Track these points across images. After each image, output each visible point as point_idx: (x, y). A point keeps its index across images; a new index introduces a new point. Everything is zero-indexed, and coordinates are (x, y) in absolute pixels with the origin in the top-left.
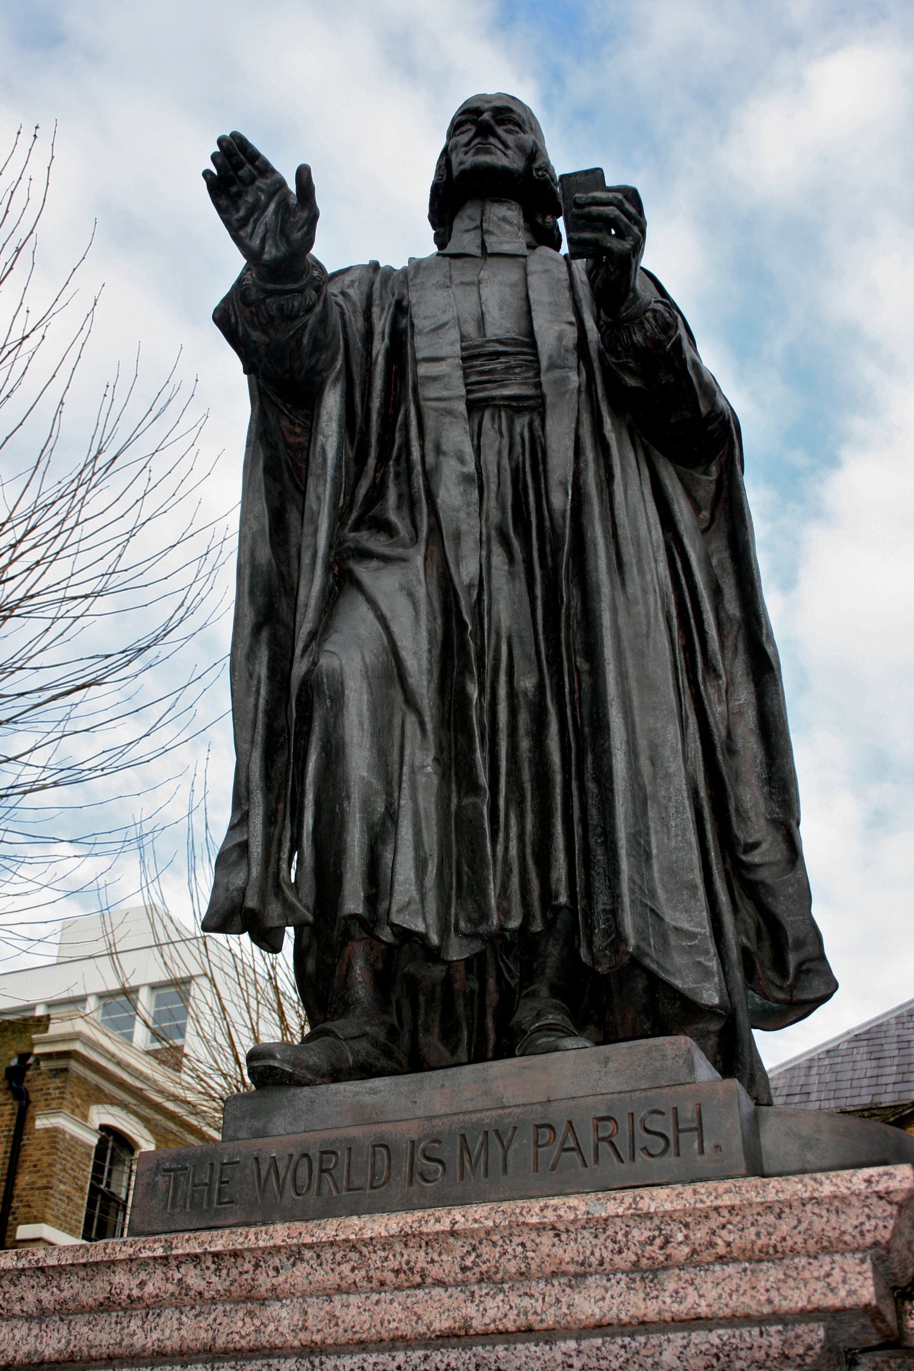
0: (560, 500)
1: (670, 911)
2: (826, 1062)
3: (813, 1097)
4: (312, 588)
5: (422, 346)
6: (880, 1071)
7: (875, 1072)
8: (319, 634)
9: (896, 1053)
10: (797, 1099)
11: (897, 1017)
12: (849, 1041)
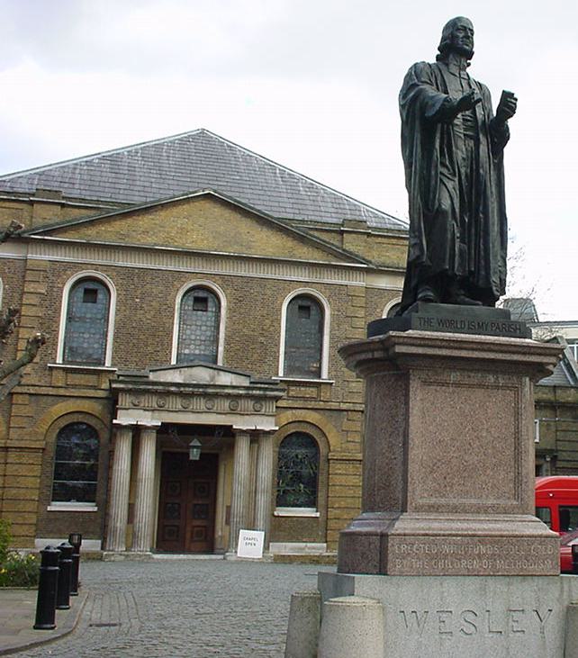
3: (77, 186)
6: (117, 181)
9: (126, 172)
11: (128, 152)
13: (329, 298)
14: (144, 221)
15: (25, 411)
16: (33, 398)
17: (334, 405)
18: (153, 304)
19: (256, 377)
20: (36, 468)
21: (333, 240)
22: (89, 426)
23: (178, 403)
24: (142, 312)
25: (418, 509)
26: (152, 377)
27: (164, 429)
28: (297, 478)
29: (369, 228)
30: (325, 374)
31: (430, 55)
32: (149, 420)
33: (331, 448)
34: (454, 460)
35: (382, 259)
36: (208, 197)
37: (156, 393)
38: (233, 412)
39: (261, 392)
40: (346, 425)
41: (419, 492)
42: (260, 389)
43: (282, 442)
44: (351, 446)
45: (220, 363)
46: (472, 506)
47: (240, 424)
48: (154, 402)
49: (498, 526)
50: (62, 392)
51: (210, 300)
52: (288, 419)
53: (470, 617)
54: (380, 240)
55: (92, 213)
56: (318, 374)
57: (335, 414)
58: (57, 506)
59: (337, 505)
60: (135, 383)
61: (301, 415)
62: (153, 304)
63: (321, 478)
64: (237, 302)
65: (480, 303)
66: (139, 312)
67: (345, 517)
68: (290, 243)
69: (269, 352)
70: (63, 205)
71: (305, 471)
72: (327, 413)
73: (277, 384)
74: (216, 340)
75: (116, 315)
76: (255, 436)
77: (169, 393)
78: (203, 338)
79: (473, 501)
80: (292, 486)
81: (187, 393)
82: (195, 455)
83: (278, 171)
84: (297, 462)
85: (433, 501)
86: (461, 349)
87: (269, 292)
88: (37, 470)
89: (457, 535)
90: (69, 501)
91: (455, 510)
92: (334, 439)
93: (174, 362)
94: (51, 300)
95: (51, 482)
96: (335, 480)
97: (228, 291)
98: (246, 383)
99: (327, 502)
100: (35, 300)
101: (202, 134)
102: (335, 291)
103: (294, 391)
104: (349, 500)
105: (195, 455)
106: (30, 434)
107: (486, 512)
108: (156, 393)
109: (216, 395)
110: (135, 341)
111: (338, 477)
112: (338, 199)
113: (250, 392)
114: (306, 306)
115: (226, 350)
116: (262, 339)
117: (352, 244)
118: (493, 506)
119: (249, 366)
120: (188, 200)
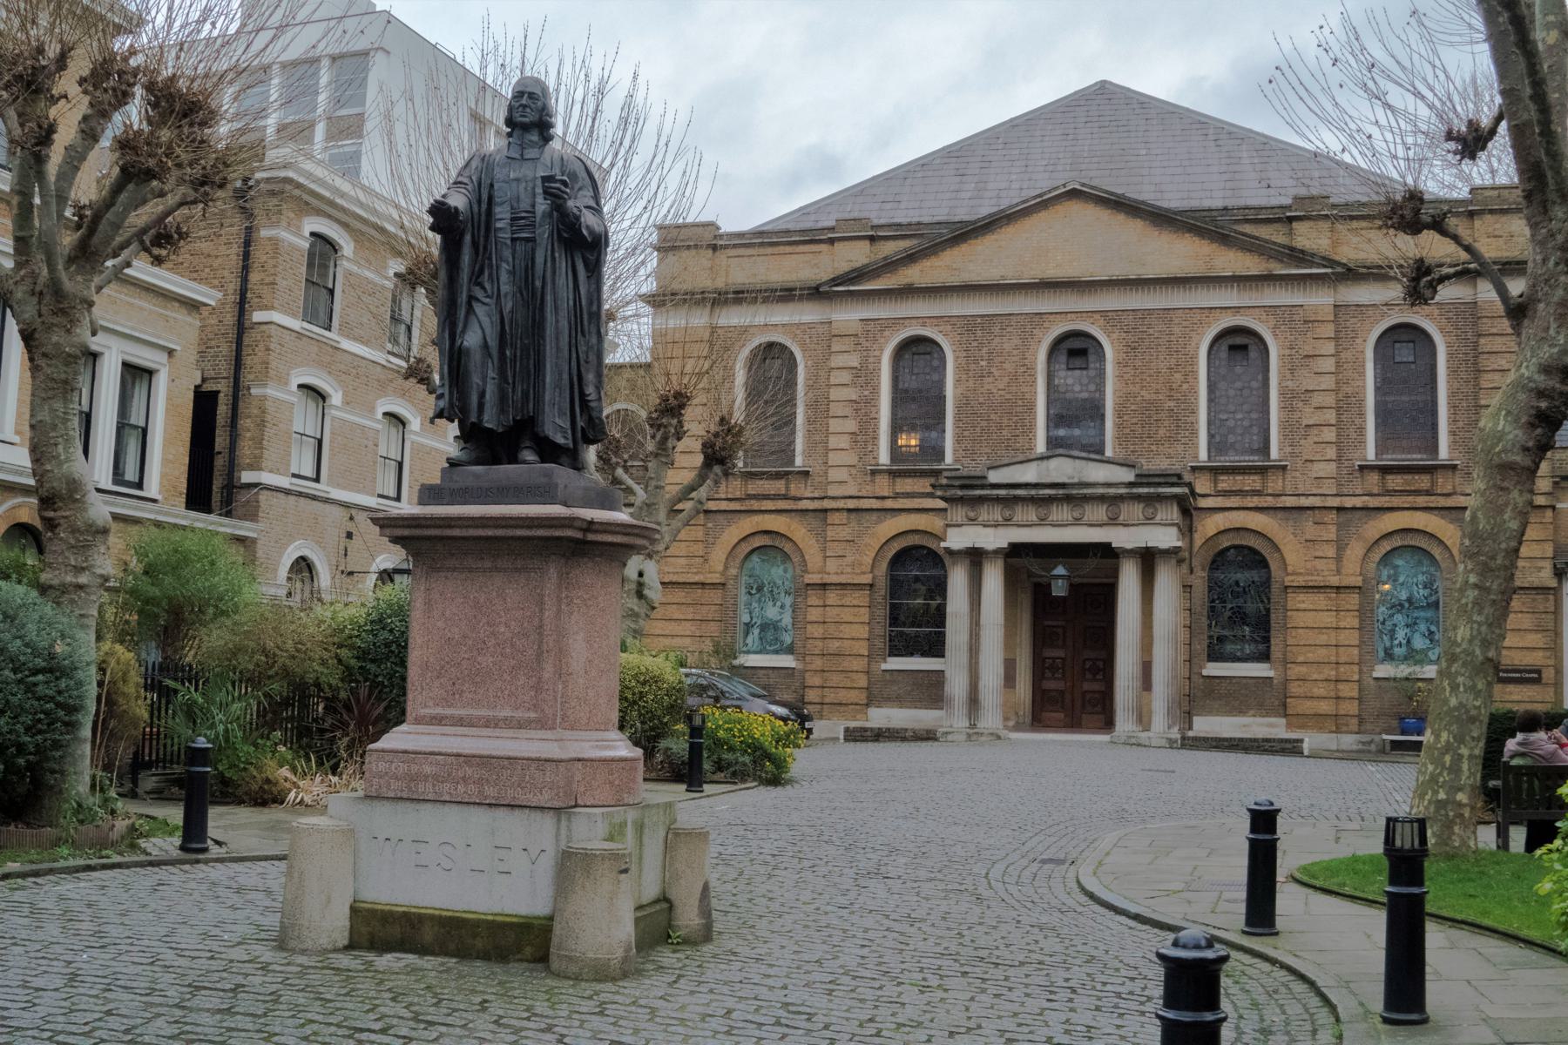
0: (538, 284)
1: (556, 426)
3: (903, 206)
4: (462, 313)
5: (497, 209)
8: (464, 331)
10: (888, 206)
15: (844, 533)
16: (853, 516)
17: (1290, 502)
19: (1160, 464)
20: (863, 610)
22: (929, 549)
23: (1031, 514)
25: (418, 721)
26: (994, 477)
27: (1016, 551)
28: (1239, 617)
29: (1334, 206)
30: (1274, 453)
32: (994, 539)
33: (1290, 569)
34: (465, 664)
36: (1074, 194)
37: (998, 500)
38: (1113, 521)
39: (1152, 490)
40: (1310, 530)
41: (416, 702)
42: (1149, 485)
43: (1213, 562)
44: (1320, 564)
45: (1109, 453)
47: (1121, 538)
48: (996, 514)
49: (498, 743)
50: (889, 504)
51: (1091, 351)
55: (915, 242)
57: (1295, 514)
58: (896, 663)
59: (1301, 659)
60: (962, 487)
66: (987, 380)
67: (1315, 676)
69: (1182, 425)
70: (872, 239)
71: (1251, 607)
72: (1280, 514)
75: (955, 387)
76: (1148, 559)
79: (483, 712)
81: (1046, 497)
82: (1059, 589)
83: (1211, 131)
84: (1239, 592)
85: (439, 711)
86: (450, 527)
87: (1176, 330)
88: (864, 614)
89: (440, 754)
90: (912, 655)
91: (460, 722)
93: (1041, 447)
94: (864, 376)
95: (882, 629)
96: (1298, 619)
97: (1115, 336)
100: (845, 377)
103: (1226, 482)
104: (1323, 651)
105: (1059, 589)
106: (853, 565)
107: (496, 726)
108: (998, 500)
109: (1086, 499)
110: (984, 424)
113: (1135, 490)
116: (1172, 404)
117: (1309, 237)
118: (506, 719)
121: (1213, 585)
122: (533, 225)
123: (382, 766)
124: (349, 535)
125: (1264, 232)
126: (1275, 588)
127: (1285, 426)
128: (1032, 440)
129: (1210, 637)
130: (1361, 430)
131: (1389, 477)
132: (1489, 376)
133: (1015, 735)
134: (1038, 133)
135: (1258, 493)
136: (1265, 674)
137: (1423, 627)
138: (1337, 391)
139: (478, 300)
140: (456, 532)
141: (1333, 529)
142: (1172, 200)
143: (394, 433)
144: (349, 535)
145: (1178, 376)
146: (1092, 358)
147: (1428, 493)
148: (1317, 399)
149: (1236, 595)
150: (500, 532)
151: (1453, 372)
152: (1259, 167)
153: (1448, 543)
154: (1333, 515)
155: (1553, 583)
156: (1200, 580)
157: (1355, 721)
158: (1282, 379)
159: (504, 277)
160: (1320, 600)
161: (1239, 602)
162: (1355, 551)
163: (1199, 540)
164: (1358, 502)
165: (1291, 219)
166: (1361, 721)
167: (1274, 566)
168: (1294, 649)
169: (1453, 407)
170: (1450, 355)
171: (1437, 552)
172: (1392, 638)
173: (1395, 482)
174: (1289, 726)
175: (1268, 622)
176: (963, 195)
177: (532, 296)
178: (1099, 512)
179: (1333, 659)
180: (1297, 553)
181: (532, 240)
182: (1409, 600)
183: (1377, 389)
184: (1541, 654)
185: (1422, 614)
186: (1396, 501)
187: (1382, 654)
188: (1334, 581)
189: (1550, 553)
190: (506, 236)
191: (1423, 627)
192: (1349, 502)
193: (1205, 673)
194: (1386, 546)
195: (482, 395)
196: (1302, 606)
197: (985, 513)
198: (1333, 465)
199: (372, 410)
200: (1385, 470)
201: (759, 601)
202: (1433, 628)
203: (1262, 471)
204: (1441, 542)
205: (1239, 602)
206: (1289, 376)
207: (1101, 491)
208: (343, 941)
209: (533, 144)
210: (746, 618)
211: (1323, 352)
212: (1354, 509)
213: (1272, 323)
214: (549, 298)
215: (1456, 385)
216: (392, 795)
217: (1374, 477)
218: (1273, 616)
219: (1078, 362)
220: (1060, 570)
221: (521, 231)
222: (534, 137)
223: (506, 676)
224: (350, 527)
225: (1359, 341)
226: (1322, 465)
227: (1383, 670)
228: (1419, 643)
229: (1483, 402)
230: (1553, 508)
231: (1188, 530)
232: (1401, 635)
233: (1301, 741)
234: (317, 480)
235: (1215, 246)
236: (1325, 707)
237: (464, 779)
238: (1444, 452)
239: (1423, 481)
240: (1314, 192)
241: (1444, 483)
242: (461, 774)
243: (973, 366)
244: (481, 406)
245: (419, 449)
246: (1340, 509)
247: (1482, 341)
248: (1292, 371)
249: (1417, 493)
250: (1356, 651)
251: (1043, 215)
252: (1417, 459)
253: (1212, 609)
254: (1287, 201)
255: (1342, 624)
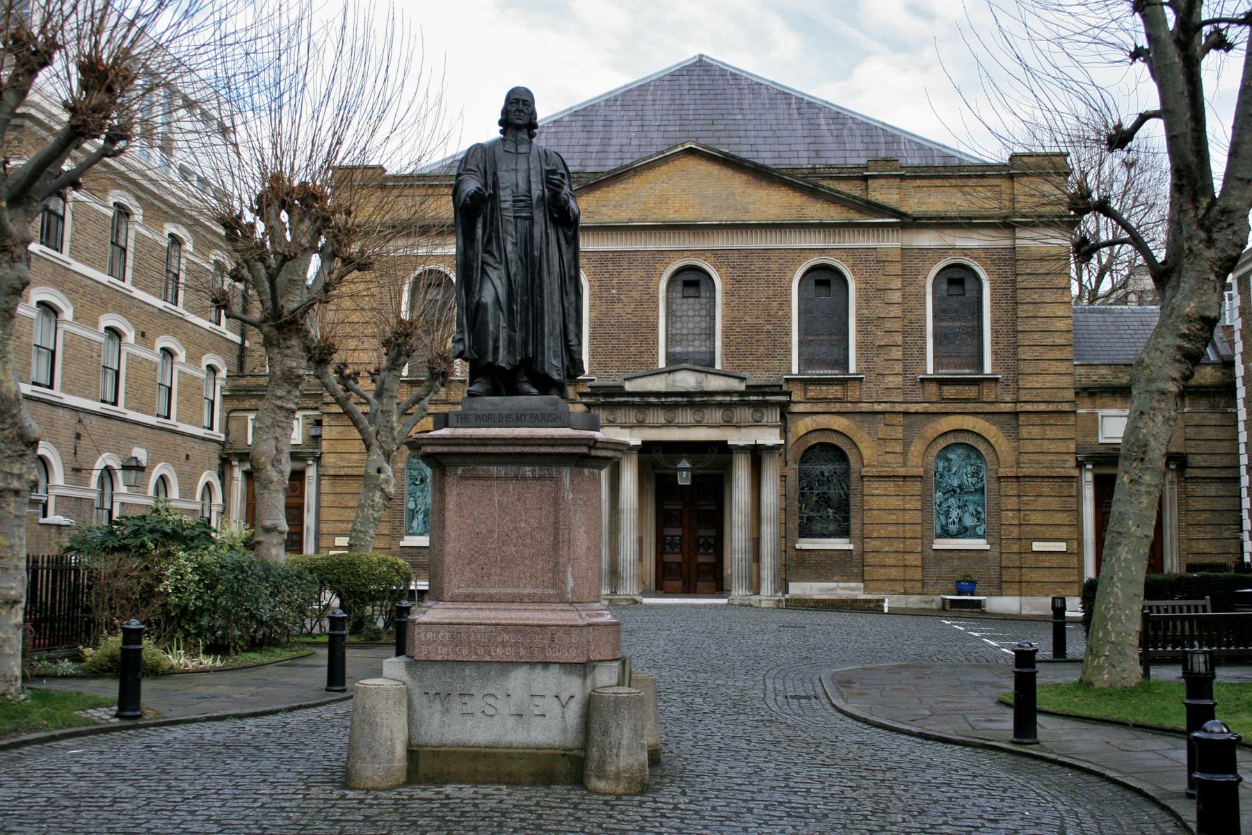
0: (536, 253)
1: (553, 365)
2: (552, 130)
5: (502, 193)
7: (585, 142)
8: (480, 290)
9: (601, 129)
12: (570, 115)
13: (853, 268)
14: (615, 193)
17: (865, 407)
18: (634, 294)
21: (851, 189)
23: (660, 417)
24: (620, 305)
25: (453, 600)
26: (629, 386)
27: (647, 446)
28: (824, 501)
30: (853, 368)
31: (490, 131)
33: (866, 462)
34: (491, 552)
35: (924, 208)
36: (691, 152)
38: (728, 424)
40: (882, 431)
41: (455, 583)
42: (757, 394)
43: (803, 456)
44: (890, 458)
45: (718, 366)
46: (506, 595)
47: (736, 438)
48: (632, 416)
49: (527, 614)
51: (703, 282)
52: (807, 426)
53: (491, 700)
54: (918, 182)
56: (845, 365)
57: (870, 418)
59: (875, 535)
61: (823, 421)
62: (634, 294)
63: (854, 501)
64: (735, 282)
65: (534, 390)
68: (797, 199)
71: (834, 492)
72: (858, 418)
73: (781, 386)
74: (711, 335)
75: (591, 311)
76: (757, 454)
77: (649, 405)
78: (697, 331)
79: (509, 590)
80: (818, 511)
82: (684, 479)
83: (793, 101)
84: (824, 480)
85: (470, 590)
86: (485, 445)
87: (774, 267)
91: (490, 599)
92: (868, 449)
93: (662, 364)
96: (874, 503)
97: (723, 270)
98: (742, 387)
99: (862, 530)
101: (701, 68)
102: (869, 260)
103: (813, 392)
104: (892, 528)
105: (684, 479)
110: (615, 342)
111: (875, 498)
112: (871, 131)
114: (825, 279)
115: (725, 345)
116: (770, 327)
117: (882, 193)
119: (755, 363)
120: (665, 160)
121: (803, 475)
122: (530, 206)
123: (430, 635)
124: (78, 436)
125: (843, 187)
126: (854, 477)
127: (860, 345)
128: (655, 356)
129: (801, 518)
130: (923, 350)
131: (945, 388)
132: (1025, 307)
133: (646, 601)
134: (650, 98)
135: (837, 400)
136: (846, 547)
137: (971, 508)
138: (903, 318)
139: (488, 264)
140: (490, 449)
141: (900, 429)
142: (767, 159)
143: (113, 346)
144: (78, 436)
145: (774, 304)
146: (703, 288)
147: (976, 401)
148: (888, 325)
149: (821, 484)
150: (527, 449)
151: (995, 303)
152: (835, 133)
153: (992, 441)
154: (900, 418)
155: (1075, 473)
156: (792, 471)
157: (919, 584)
158: (859, 308)
159: (509, 247)
160: (891, 487)
161: (825, 490)
162: (917, 448)
163: (792, 440)
164: (920, 408)
165: (865, 179)
166: (924, 584)
167: (853, 459)
168: (870, 527)
169: (995, 332)
170: (993, 290)
171: (982, 448)
172: (947, 517)
173: (949, 391)
174: (866, 589)
175: (848, 505)
176: (590, 149)
177: (532, 265)
178: (717, 415)
179: (901, 535)
180: (869, 451)
181: (531, 219)
182: (960, 486)
183: (935, 317)
184: (1066, 529)
185: (971, 498)
186: (951, 407)
187: (939, 531)
188: (902, 471)
189: (1072, 447)
190: (509, 214)
191: (971, 508)
192: (913, 408)
193: (798, 546)
194: (942, 443)
195: (496, 340)
196: (876, 492)
197: (621, 416)
198: (900, 379)
199: (95, 324)
200: (942, 382)
201: (422, 491)
202: (980, 509)
203: (843, 382)
204: (986, 440)
205: (825, 490)
206: (864, 306)
207: (719, 398)
208: (403, 779)
209: (523, 141)
210: (411, 505)
211: (892, 286)
212: (916, 413)
213: (851, 262)
214: (545, 265)
215: (998, 314)
216: (439, 658)
217: (932, 389)
218: (852, 501)
219: (691, 291)
220: (685, 464)
221: (521, 211)
222: (523, 135)
223: (527, 562)
224: (79, 428)
225: (920, 278)
226: (891, 378)
227: (941, 544)
228: (969, 521)
229: (1020, 328)
230: (1074, 412)
231: (784, 432)
232: (954, 515)
233: (883, 601)
234: (51, 387)
235: (805, 198)
236: (894, 573)
237: (503, 644)
238: (988, 368)
239: (971, 391)
240: (882, 154)
241: (989, 393)
242: (499, 639)
243: (605, 294)
244: (496, 349)
245: (132, 359)
246: (905, 413)
247: (1019, 279)
248: (867, 301)
249: (967, 401)
250: (919, 528)
251: (664, 168)
252: (967, 373)
253: (802, 495)
254: (863, 161)
255: (908, 506)
